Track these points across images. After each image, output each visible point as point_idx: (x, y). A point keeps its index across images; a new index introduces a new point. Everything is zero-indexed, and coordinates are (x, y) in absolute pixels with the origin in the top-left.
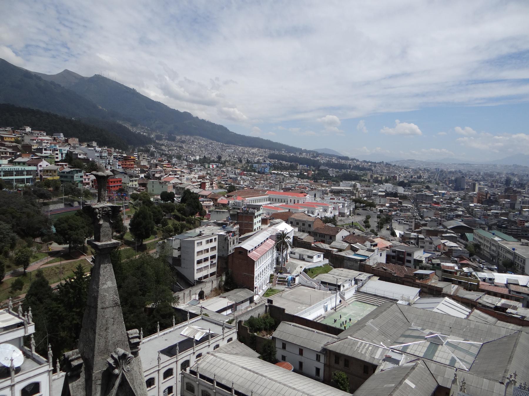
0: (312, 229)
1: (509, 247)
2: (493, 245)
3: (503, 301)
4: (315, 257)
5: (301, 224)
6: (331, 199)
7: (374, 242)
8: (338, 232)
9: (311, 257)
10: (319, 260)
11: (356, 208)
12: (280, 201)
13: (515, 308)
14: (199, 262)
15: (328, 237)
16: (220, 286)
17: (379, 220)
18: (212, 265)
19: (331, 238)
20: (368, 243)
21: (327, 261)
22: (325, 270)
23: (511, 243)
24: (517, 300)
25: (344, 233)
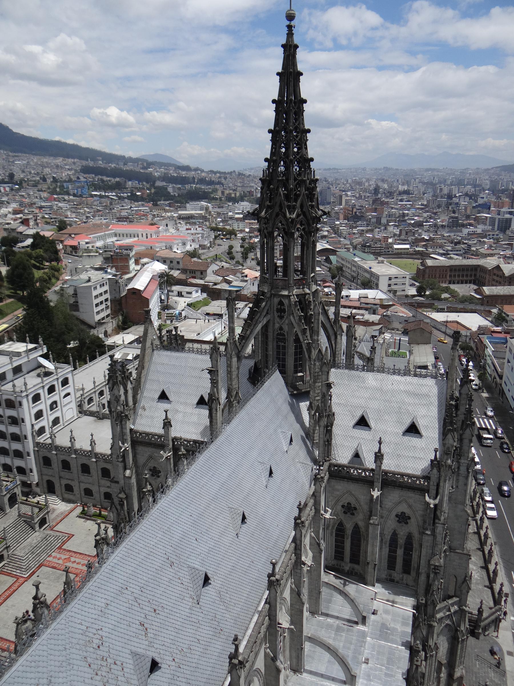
0: (181, 266)
1: (366, 266)
2: (354, 265)
3: (354, 311)
4: (194, 293)
5: (168, 262)
6: (187, 229)
7: (244, 273)
8: (208, 267)
9: (190, 293)
10: (197, 295)
11: (216, 237)
12: (132, 236)
13: (363, 315)
14: (97, 305)
15: (199, 273)
16: (118, 326)
17: (242, 249)
18: (107, 308)
19: (202, 273)
20: (239, 275)
21: (205, 295)
22: (205, 303)
23: (369, 262)
24: (366, 309)
25: (214, 267)
